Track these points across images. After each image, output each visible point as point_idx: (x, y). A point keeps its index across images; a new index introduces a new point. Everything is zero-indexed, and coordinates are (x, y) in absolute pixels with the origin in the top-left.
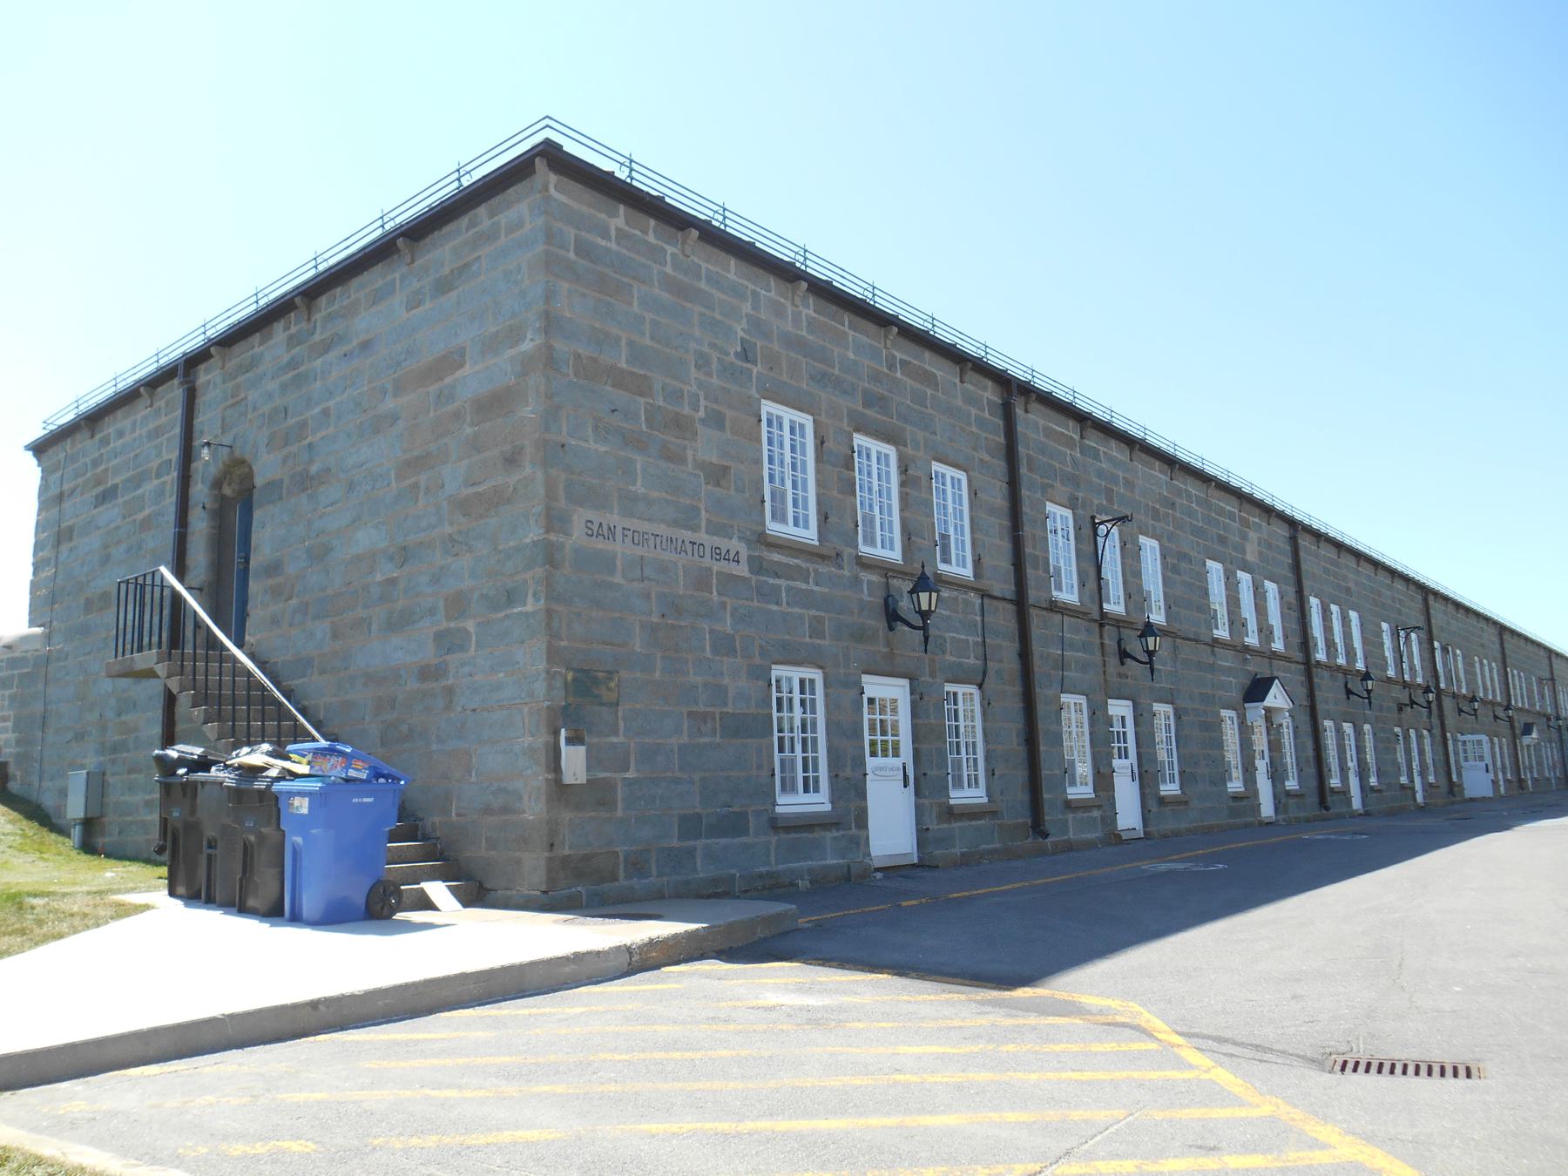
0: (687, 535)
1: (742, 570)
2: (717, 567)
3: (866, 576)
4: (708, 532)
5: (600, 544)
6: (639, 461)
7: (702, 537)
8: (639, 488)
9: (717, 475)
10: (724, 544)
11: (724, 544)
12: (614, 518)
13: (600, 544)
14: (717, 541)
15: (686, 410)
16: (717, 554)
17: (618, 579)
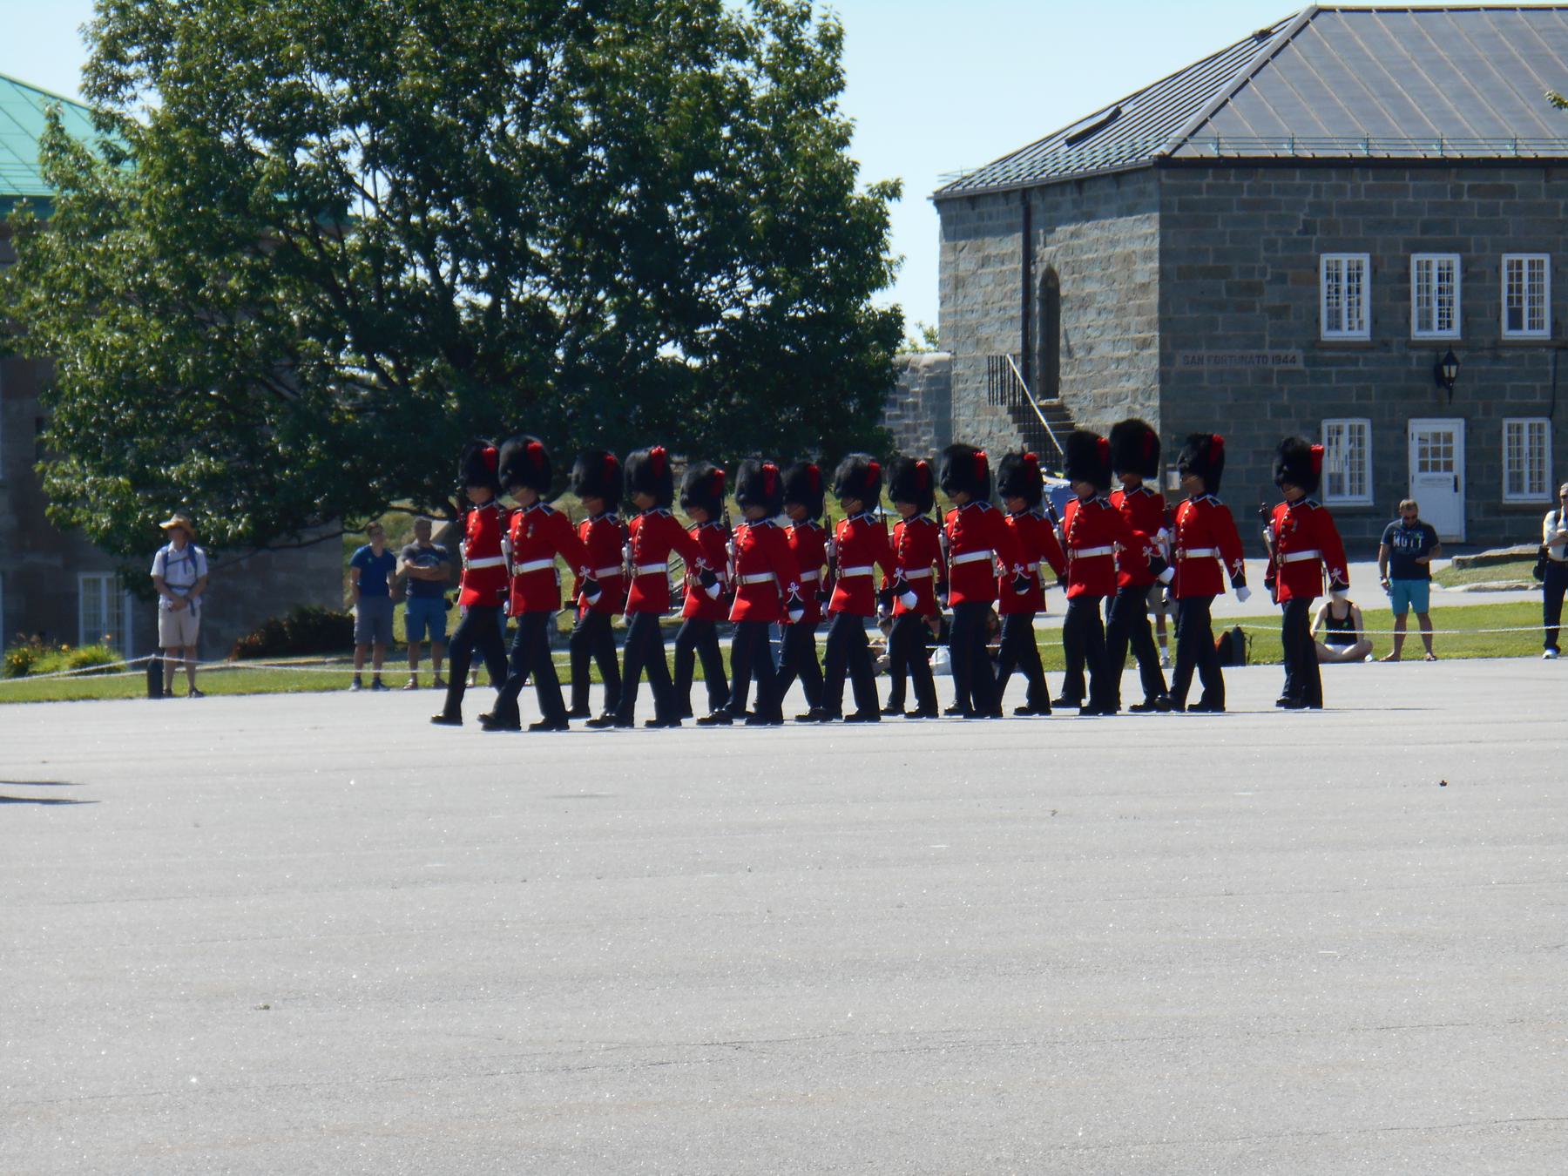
0: (1255, 352)
1: (1300, 365)
2: (1276, 368)
3: (1414, 354)
4: (1271, 347)
5: (1194, 368)
6: (1220, 317)
7: (1267, 351)
8: (1220, 332)
9: (1279, 312)
10: (1282, 353)
11: (1282, 353)
12: (1203, 352)
13: (1194, 368)
14: (1277, 352)
15: (1257, 278)
16: (1277, 359)
17: (1205, 383)
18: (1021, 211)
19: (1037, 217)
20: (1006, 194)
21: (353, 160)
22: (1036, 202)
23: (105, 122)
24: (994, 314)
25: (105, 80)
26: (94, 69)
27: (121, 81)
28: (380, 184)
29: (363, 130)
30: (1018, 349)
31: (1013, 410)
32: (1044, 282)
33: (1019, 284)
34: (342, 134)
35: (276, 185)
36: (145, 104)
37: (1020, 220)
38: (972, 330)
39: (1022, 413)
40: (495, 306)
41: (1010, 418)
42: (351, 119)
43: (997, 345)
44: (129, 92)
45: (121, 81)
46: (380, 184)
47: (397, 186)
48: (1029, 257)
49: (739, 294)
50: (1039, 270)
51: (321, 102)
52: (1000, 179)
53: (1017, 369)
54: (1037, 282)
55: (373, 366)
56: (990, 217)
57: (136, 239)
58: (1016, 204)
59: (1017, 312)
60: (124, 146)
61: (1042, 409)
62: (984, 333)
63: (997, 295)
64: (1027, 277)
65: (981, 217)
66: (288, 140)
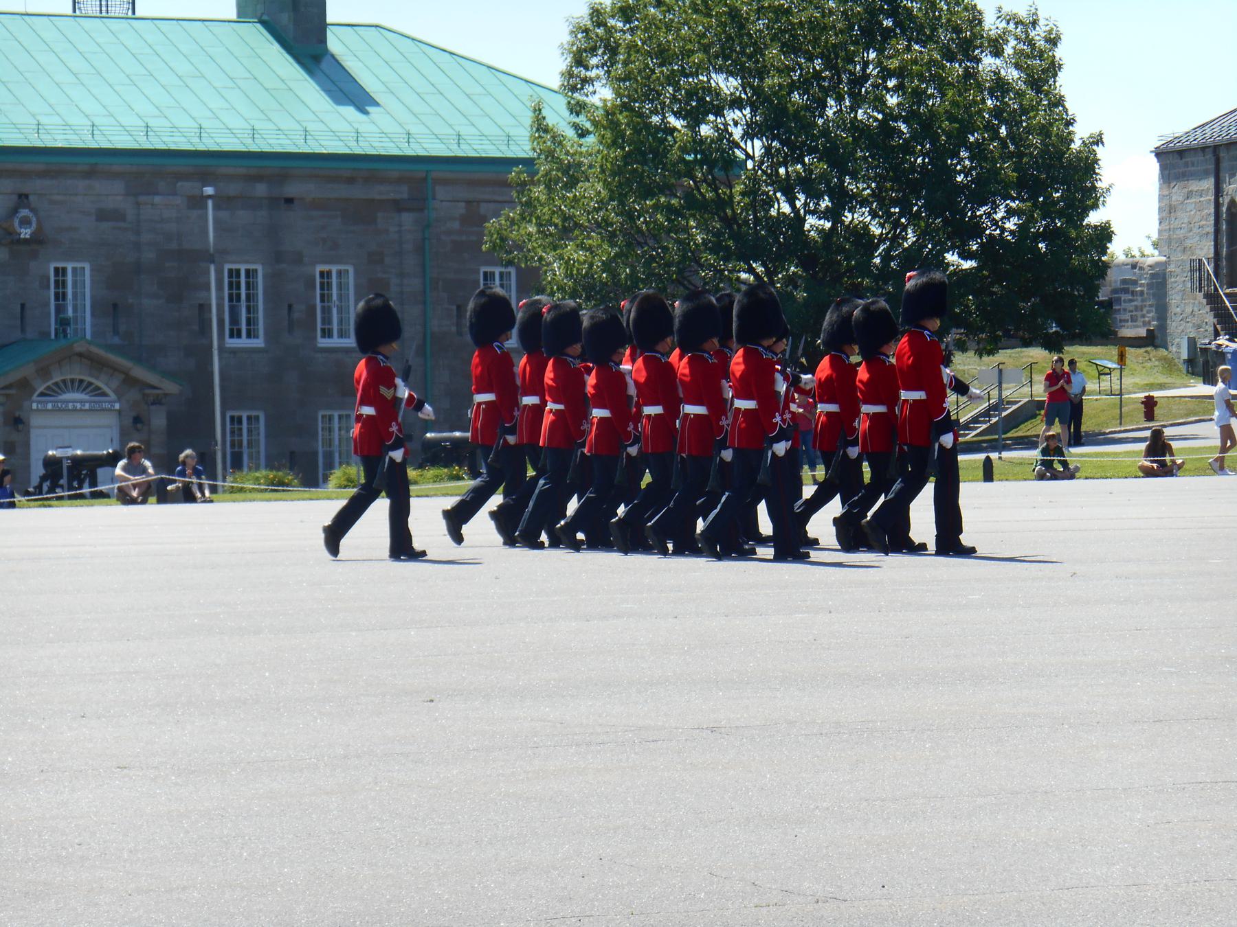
18: (1213, 159)
19: (1224, 165)
20: (1204, 149)
21: (737, 133)
22: (1222, 154)
23: (577, 108)
24: (1195, 230)
25: (574, 83)
26: (570, 74)
27: (586, 81)
28: (757, 147)
29: (747, 111)
30: (1212, 255)
31: (1207, 296)
32: (1229, 209)
33: (1212, 210)
34: (732, 115)
35: (684, 150)
36: (602, 94)
37: (1212, 167)
38: (1181, 241)
39: (1213, 299)
40: (833, 228)
41: (1204, 301)
42: (736, 103)
43: (1198, 252)
44: (591, 89)
45: (586, 81)
46: (757, 147)
47: (768, 149)
48: (1218, 191)
49: (1003, 217)
50: (1225, 201)
51: (717, 93)
52: (1199, 139)
53: (1210, 268)
54: (1224, 209)
55: (751, 270)
56: (1193, 165)
57: (592, 189)
58: (1209, 156)
59: (1211, 229)
60: (588, 125)
61: (1227, 295)
62: (1188, 243)
63: (1197, 218)
64: (1217, 205)
65: (1186, 165)
66: (694, 119)
